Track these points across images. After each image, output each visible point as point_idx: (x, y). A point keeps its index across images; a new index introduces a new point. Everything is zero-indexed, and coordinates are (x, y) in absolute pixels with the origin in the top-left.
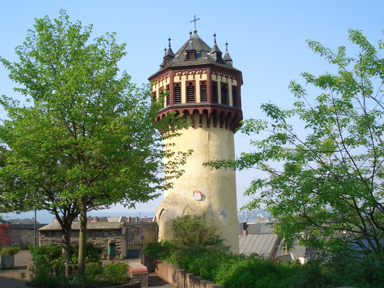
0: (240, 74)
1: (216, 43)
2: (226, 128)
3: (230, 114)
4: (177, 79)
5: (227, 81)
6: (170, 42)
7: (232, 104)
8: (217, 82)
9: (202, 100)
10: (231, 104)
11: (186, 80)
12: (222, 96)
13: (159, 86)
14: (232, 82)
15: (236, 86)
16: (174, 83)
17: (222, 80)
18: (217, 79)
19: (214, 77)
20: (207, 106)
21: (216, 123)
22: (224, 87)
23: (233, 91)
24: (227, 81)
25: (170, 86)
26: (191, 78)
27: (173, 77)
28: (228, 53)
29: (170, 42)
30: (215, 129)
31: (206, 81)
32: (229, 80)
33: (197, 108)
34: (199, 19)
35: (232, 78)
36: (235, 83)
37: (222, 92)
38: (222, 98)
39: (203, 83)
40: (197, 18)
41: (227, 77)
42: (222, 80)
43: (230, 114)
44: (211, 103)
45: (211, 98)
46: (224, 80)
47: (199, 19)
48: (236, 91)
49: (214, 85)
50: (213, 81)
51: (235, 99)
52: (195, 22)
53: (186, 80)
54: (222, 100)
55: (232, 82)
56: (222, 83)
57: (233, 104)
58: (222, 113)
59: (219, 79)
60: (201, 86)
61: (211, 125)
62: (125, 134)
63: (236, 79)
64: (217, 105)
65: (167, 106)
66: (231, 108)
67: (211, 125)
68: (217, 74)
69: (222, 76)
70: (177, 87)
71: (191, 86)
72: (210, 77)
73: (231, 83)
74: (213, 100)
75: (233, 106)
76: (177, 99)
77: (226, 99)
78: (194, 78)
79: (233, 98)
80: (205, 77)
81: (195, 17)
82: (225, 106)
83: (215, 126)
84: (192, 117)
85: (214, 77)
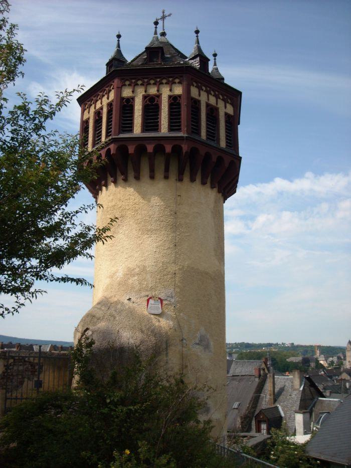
0: (239, 96)
1: (198, 43)
2: (212, 187)
3: (220, 159)
4: (127, 93)
5: (217, 104)
6: (119, 41)
7: (225, 145)
8: (199, 101)
9: (171, 128)
10: (223, 144)
11: (144, 93)
12: (207, 128)
13: (95, 108)
14: (226, 107)
15: (232, 116)
16: (123, 99)
17: (208, 99)
18: (200, 95)
19: (194, 92)
20: (181, 138)
21: (196, 174)
22: (212, 112)
23: (226, 122)
24: (217, 104)
25: (114, 104)
26: (153, 91)
27: (121, 88)
28: (217, 69)
29: (119, 41)
30: (193, 185)
31: (180, 96)
32: (221, 104)
33: (162, 142)
34: (169, 15)
35: (225, 101)
36: (230, 110)
37: (207, 121)
38: (207, 131)
39: (174, 101)
40: (166, 13)
41: (217, 97)
42: (208, 99)
43: (220, 159)
44: (188, 133)
45: (187, 126)
46: (212, 100)
47: (169, 15)
48: (233, 122)
49: (195, 105)
50: (192, 99)
51: (230, 144)
52: (163, 20)
53: (144, 93)
54: (207, 135)
55: (226, 107)
56: (208, 105)
57: (227, 145)
58: (208, 156)
59: (204, 98)
60: (171, 106)
61: (186, 179)
62: (18, 142)
63: (232, 104)
64: (199, 139)
65: (106, 139)
66: (222, 150)
67: (186, 179)
68: (200, 89)
69: (208, 93)
70: (127, 106)
71: (152, 105)
72: (188, 91)
73: (224, 109)
74: (192, 132)
75: (226, 148)
76: (126, 123)
77: (214, 134)
78: (158, 91)
79: (227, 136)
80: (178, 90)
81: (163, 12)
82: (212, 143)
83: (193, 180)
84: (152, 158)
85: (194, 92)
